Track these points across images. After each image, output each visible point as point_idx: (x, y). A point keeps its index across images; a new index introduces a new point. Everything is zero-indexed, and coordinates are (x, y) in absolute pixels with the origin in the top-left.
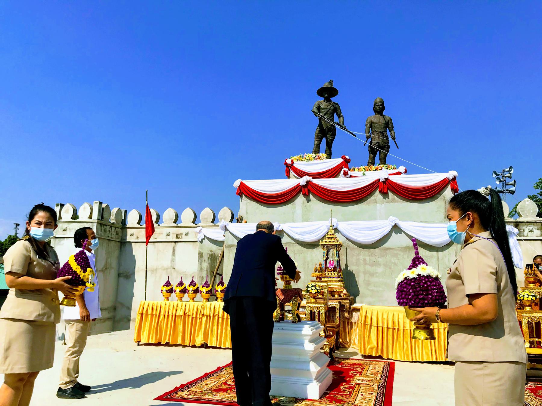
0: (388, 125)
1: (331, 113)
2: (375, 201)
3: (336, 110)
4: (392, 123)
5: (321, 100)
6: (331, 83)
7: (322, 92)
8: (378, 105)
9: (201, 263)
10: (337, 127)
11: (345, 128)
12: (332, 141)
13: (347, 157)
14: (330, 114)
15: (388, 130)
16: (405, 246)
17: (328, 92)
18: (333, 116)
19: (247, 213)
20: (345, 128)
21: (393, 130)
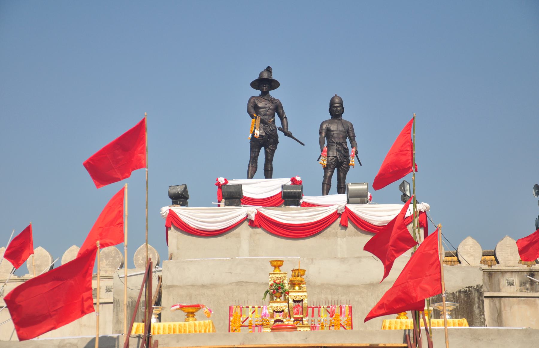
0: (349, 133)
1: (271, 114)
2: (336, 235)
3: (278, 109)
4: (353, 130)
5: (258, 93)
6: (269, 69)
7: (257, 84)
8: (336, 107)
9: (117, 313)
10: (280, 134)
11: (290, 136)
12: (273, 151)
13: (298, 178)
14: (269, 116)
15: (348, 140)
16: (369, 282)
17: (265, 83)
18: (274, 116)
19: (178, 249)
20: (290, 136)
21: (354, 140)
